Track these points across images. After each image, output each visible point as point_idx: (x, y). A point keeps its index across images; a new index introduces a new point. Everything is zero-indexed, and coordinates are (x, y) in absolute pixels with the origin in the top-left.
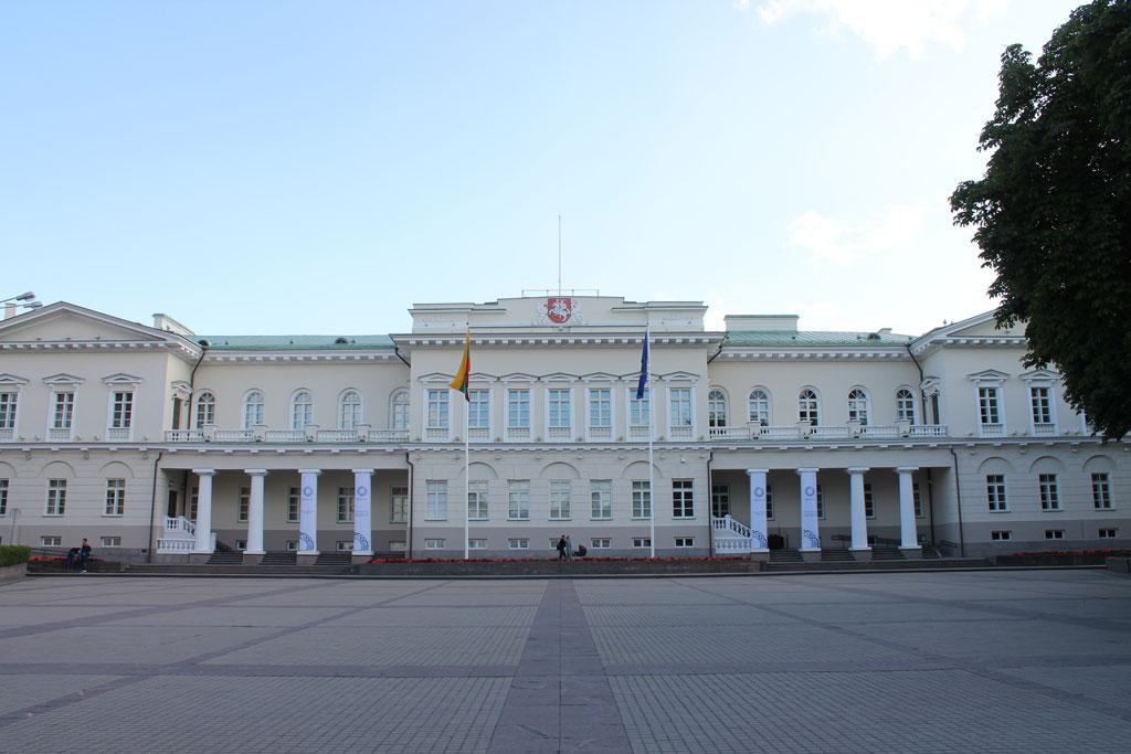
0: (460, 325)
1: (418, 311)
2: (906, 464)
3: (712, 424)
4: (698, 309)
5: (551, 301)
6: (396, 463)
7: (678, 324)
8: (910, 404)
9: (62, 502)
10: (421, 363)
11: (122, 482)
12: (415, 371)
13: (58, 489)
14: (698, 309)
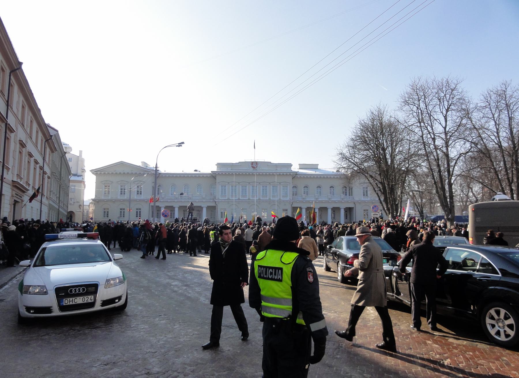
0: (229, 170)
1: (219, 165)
2: (343, 206)
3: (293, 195)
4: (290, 165)
5: (252, 163)
6: (213, 204)
7: (285, 170)
8: (346, 190)
9: (124, 214)
10: (218, 179)
11: (140, 209)
12: (217, 181)
13: (122, 211)
14: (290, 165)
